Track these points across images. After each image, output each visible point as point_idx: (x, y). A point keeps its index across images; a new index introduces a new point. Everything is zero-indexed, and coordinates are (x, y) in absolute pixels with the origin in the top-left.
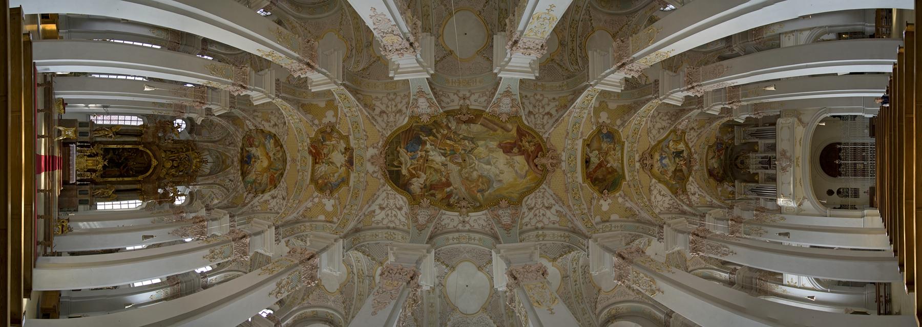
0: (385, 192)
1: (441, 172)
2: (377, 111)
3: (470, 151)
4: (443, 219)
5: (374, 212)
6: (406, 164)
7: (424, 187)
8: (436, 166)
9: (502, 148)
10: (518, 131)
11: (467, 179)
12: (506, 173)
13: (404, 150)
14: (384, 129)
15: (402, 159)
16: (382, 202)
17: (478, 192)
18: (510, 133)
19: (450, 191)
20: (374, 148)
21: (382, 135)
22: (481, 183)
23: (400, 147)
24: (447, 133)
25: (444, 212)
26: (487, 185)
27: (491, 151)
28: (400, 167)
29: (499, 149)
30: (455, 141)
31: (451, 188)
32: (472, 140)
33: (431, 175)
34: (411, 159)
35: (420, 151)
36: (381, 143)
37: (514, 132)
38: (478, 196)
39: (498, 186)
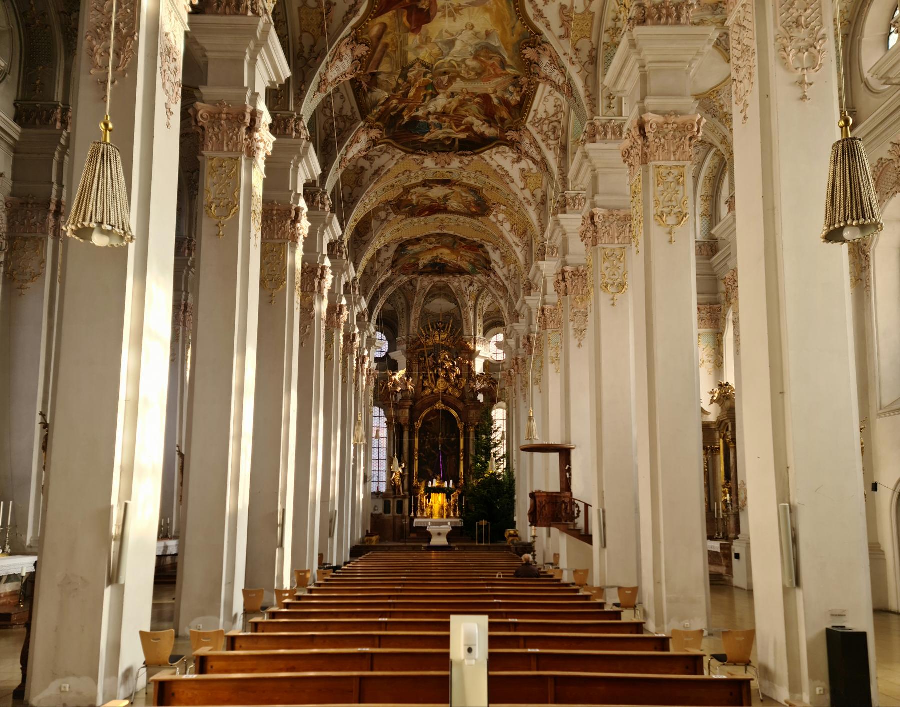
0: (494, 157)
1: (464, 100)
2: (366, 164)
3: (428, 68)
4: (546, 112)
5: (524, 170)
6: (449, 133)
7: (489, 123)
8: (455, 104)
9: (422, 25)
10: (380, 13)
11: (479, 74)
12: (472, 22)
13: (426, 135)
14: (394, 157)
15: (441, 137)
16: (509, 160)
17: (504, 69)
18: (388, 24)
19: (500, 101)
20: (423, 163)
21: (403, 159)
22: (488, 60)
23: (423, 139)
24: (398, 99)
25: (532, 114)
26: (495, 54)
27: (427, 41)
28: (454, 140)
29: (422, 30)
30: (411, 87)
31: (493, 96)
32: (405, 69)
33: (470, 111)
34: (441, 128)
35: (429, 120)
36: (415, 157)
37: (386, 18)
38: (513, 73)
39: (497, 40)
